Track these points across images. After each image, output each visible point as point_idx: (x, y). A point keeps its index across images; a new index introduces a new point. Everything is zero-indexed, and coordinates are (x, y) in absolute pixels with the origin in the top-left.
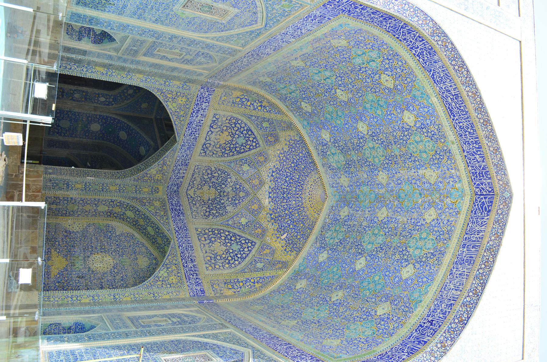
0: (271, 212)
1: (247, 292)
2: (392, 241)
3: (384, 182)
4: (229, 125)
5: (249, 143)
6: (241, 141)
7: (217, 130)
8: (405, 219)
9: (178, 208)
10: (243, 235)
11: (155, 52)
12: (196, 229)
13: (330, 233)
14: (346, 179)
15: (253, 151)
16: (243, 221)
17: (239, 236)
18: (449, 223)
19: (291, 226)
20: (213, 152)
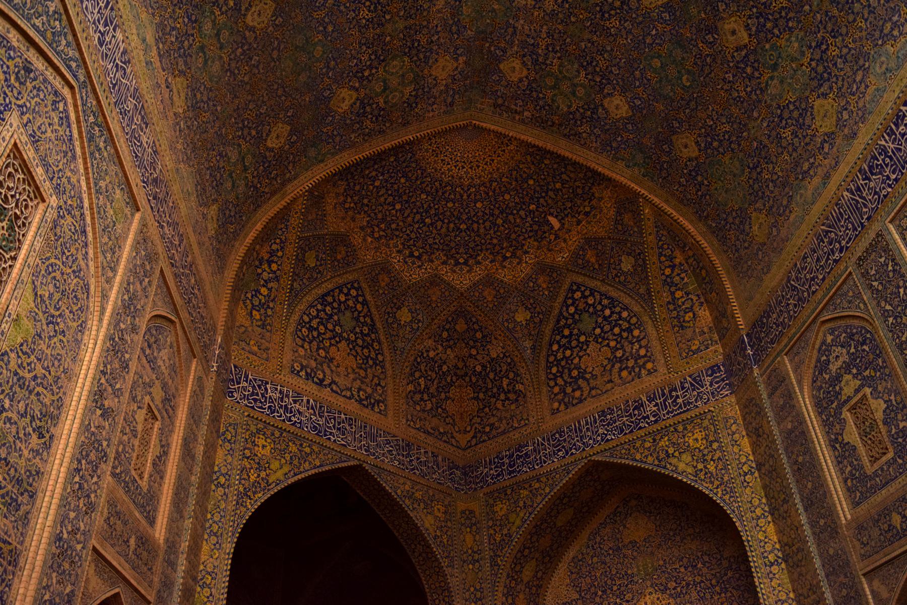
0: (500, 258)
4: (315, 343)
5: (351, 303)
6: (347, 319)
7: (328, 371)
9: (506, 461)
10: (556, 312)
11: (144, 484)
12: (555, 412)
14: (441, 62)
15: (369, 298)
16: (521, 317)
17: (558, 321)
19: (532, 207)
20: (377, 385)
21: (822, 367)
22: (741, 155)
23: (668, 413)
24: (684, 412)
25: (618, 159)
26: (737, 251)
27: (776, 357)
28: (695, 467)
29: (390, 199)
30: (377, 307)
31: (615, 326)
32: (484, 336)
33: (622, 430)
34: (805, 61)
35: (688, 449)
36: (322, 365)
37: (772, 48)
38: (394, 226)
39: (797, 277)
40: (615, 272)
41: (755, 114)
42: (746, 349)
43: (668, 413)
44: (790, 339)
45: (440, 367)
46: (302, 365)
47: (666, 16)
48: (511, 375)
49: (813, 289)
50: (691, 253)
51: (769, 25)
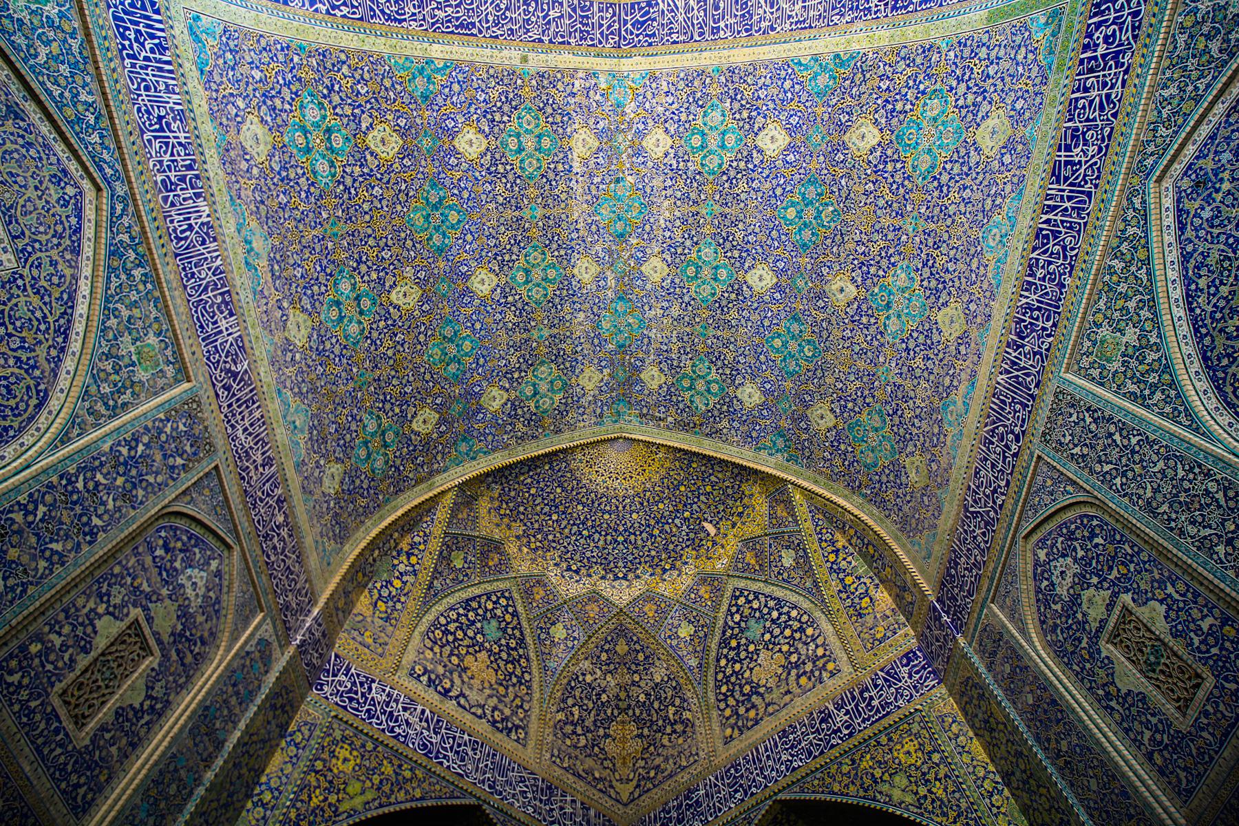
0: (658, 570)
1: (864, 555)
2: (709, 218)
3: (594, 269)
4: (448, 648)
5: (499, 612)
6: (492, 629)
7: (457, 681)
8: (666, 203)
10: (721, 622)
12: (728, 740)
13: (697, 399)
15: (520, 609)
17: (724, 633)
18: (673, 90)
19: (687, 514)
20: (517, 707)
21: (1045, 598)
22: (878, 406)
23: (863, 721)
24: (884, 716)
25: (760, 449)
26: (900, 510)
27: (981, 611)
28: (917, 793)
29: (547, 509)
30: (529, 620)
31: (786, 627)
32: (647, 658)
33: (810, 753)
34: (916, 285)
35: (901, 768)
36: (451, 673)
37: (880, 289)
38: (551, 537)
39: (975, 501)
40: (776, 570)
41: (881, 359)
42: (941, 617)
43: (863, 721)
44: (992, 579)
45: (599, 695)
46: (425, 669)
47: (777, 296)
48: (677, 702)
49: (999, 502)
50: (852, 532)
51: (873, 270)
